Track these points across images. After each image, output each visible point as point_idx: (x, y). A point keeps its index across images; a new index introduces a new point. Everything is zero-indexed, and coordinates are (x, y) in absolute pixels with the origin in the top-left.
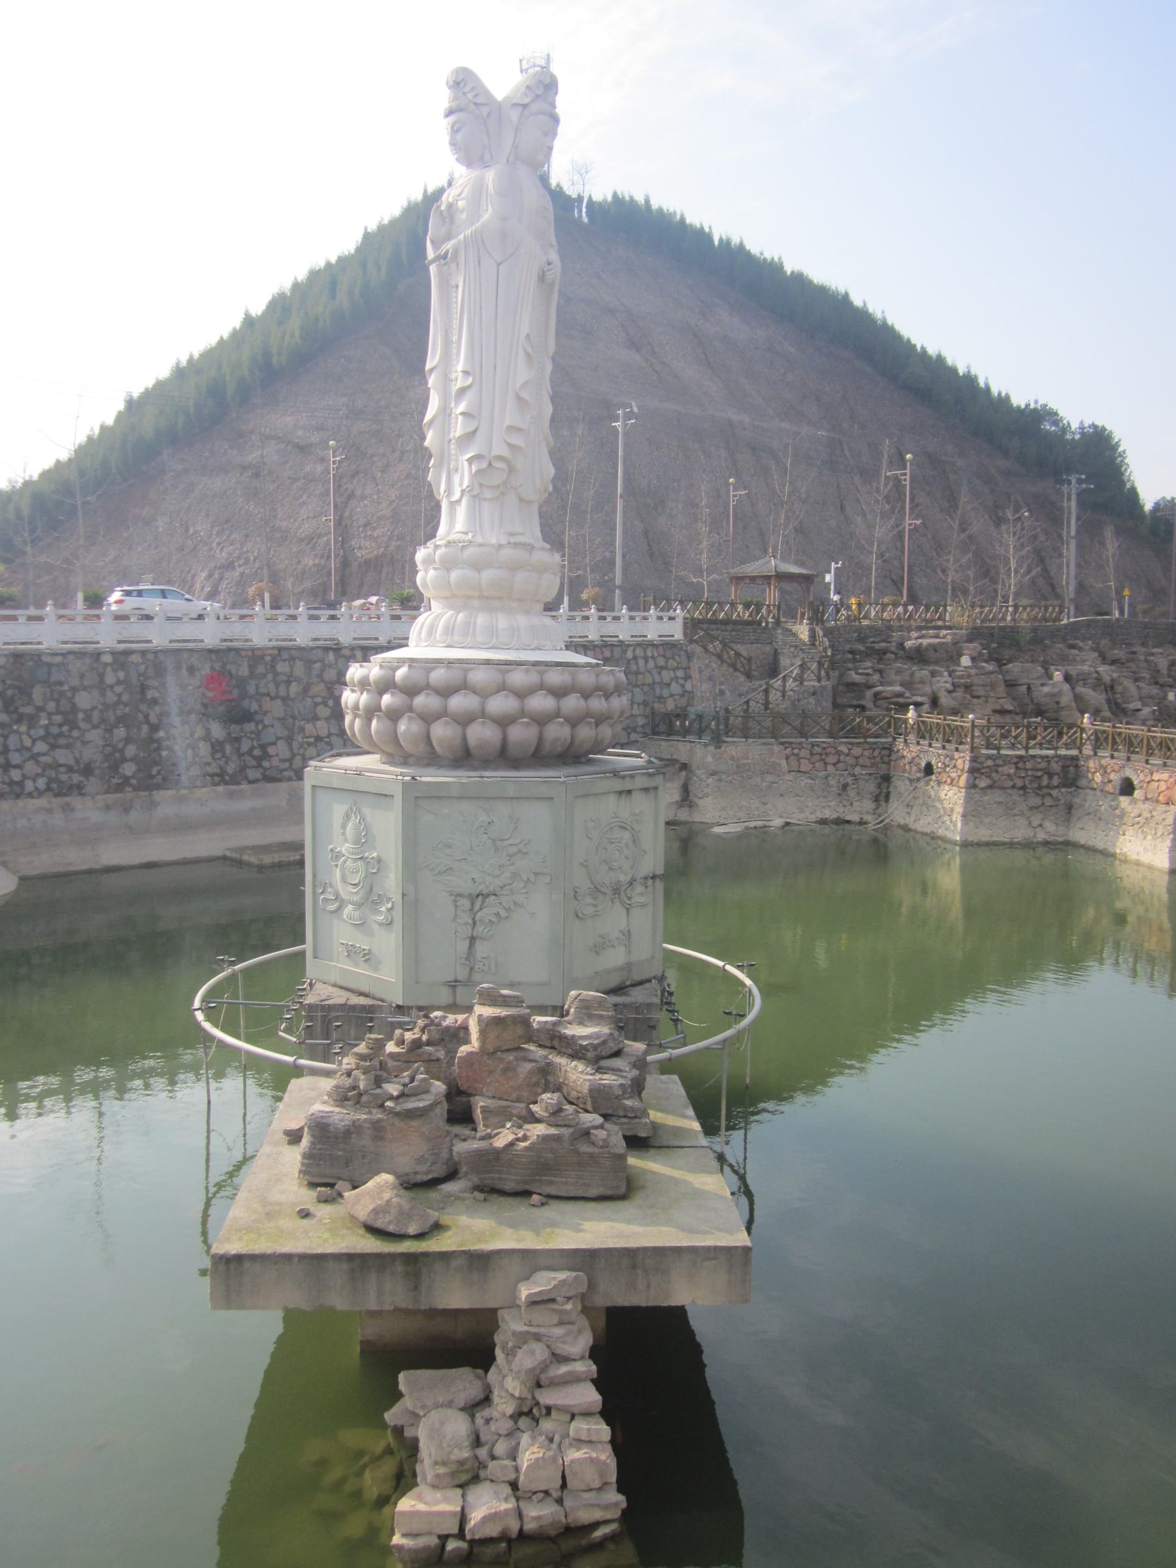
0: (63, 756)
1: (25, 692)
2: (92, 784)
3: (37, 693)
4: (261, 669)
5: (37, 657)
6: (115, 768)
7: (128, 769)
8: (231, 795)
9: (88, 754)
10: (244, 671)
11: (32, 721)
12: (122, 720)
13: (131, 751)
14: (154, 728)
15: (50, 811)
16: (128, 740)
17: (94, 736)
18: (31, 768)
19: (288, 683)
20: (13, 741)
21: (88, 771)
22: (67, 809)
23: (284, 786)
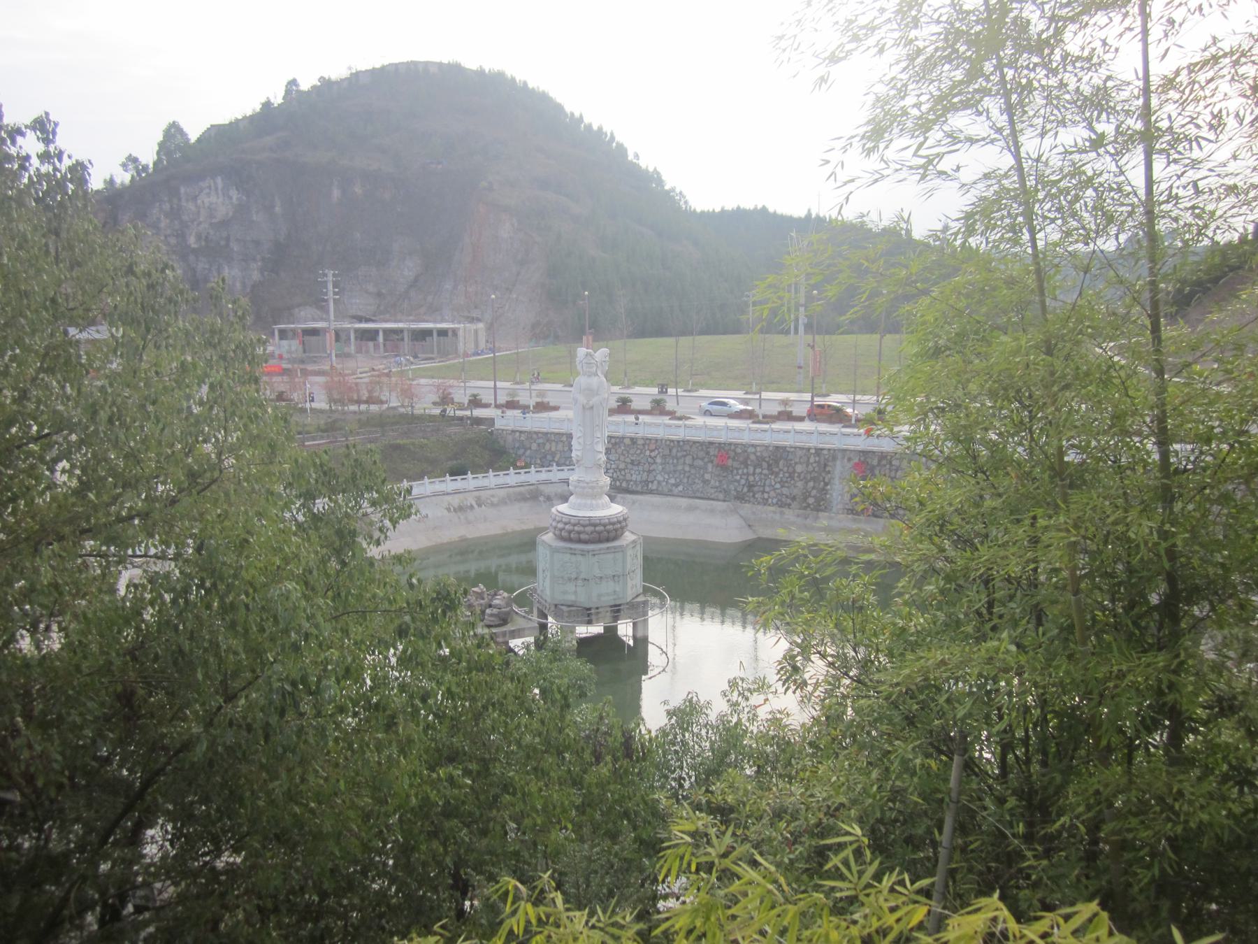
0: (785, 491)
1: (777, 462)
2: (795, 504)
3: (781, 463)
4: (884, 462)
5: (784, 448)
6: (805, 499)
7: (811, 500)
8: (854, 520)
9: (796, 492)
10: (875, 462)
11: (777, 474)
12: (813, 479)
13: (814, 492)
14: (826, 484)
15: (775, 512)
16: (813, 488)
17: (800, 484)
18: (772, 494)
19: (897, 471)
20: (768, 482)
21: (794, 499)
22: (782, 513)
23: (881, 521)
